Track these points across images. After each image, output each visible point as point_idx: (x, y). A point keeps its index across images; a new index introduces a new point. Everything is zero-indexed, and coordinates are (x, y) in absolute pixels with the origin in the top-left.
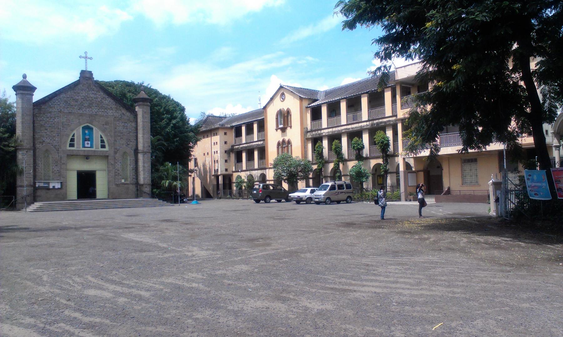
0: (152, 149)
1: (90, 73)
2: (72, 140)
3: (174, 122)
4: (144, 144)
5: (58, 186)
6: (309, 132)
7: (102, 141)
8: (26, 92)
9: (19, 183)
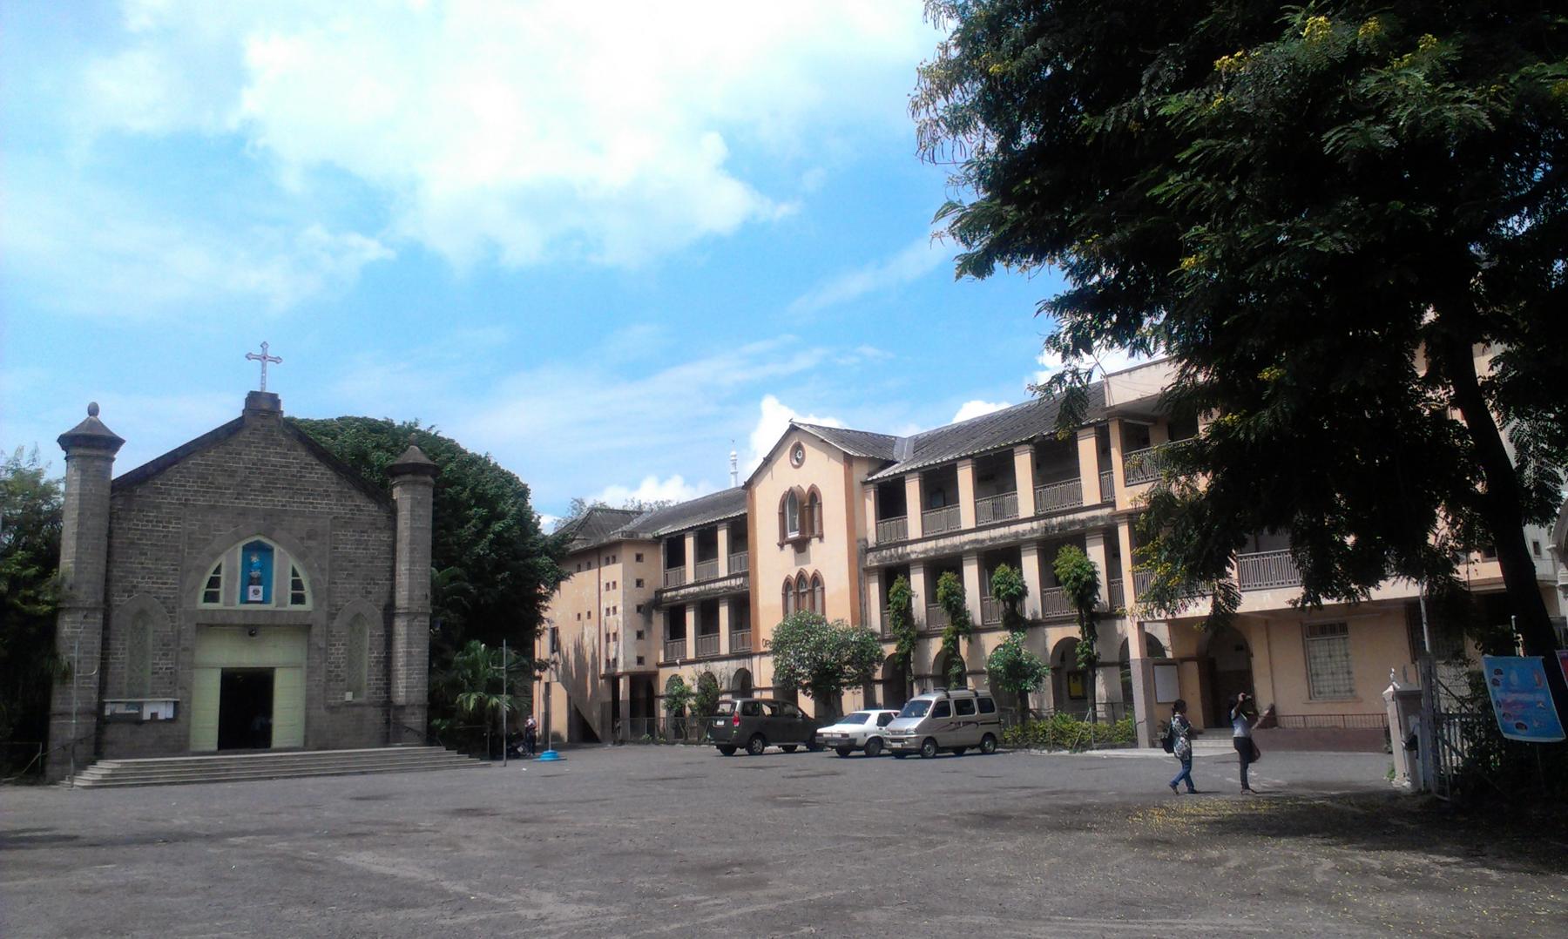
0: (432, 603)
1: (274, 399)
2: (214, 582)
3: (497, 526)
4: (411, 591)
5: (165, 712)
6: (872, 550)
7: (297, 585)
8: (95, 452)
9: (57, 705)
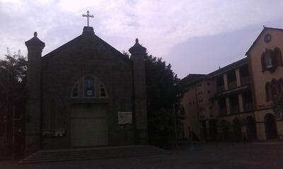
2: (76, 90)
7: (102, 90)
